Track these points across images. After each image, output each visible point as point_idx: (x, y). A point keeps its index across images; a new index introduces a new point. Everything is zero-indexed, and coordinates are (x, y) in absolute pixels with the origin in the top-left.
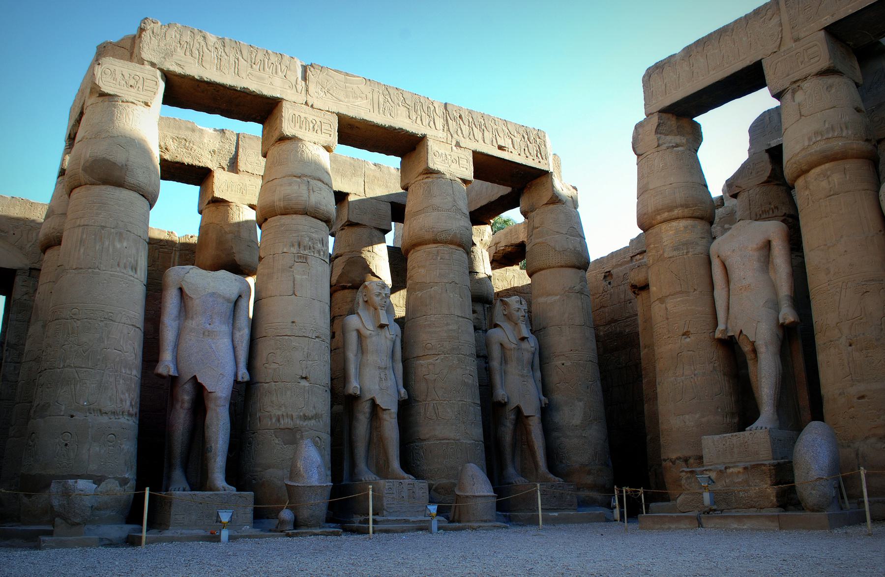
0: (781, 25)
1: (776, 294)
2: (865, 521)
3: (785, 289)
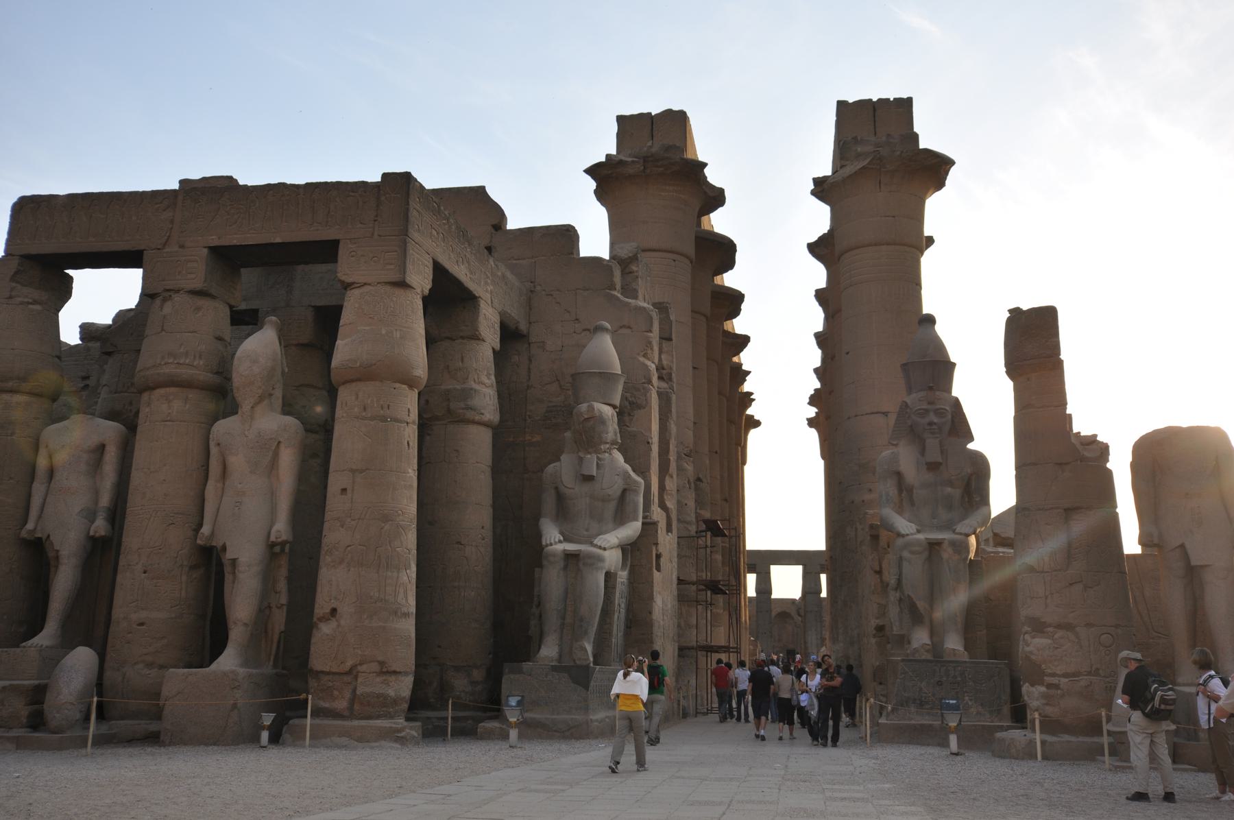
0: (172, 222)
1: (96, 502)
2: (86, 746)
3: (105, 500)
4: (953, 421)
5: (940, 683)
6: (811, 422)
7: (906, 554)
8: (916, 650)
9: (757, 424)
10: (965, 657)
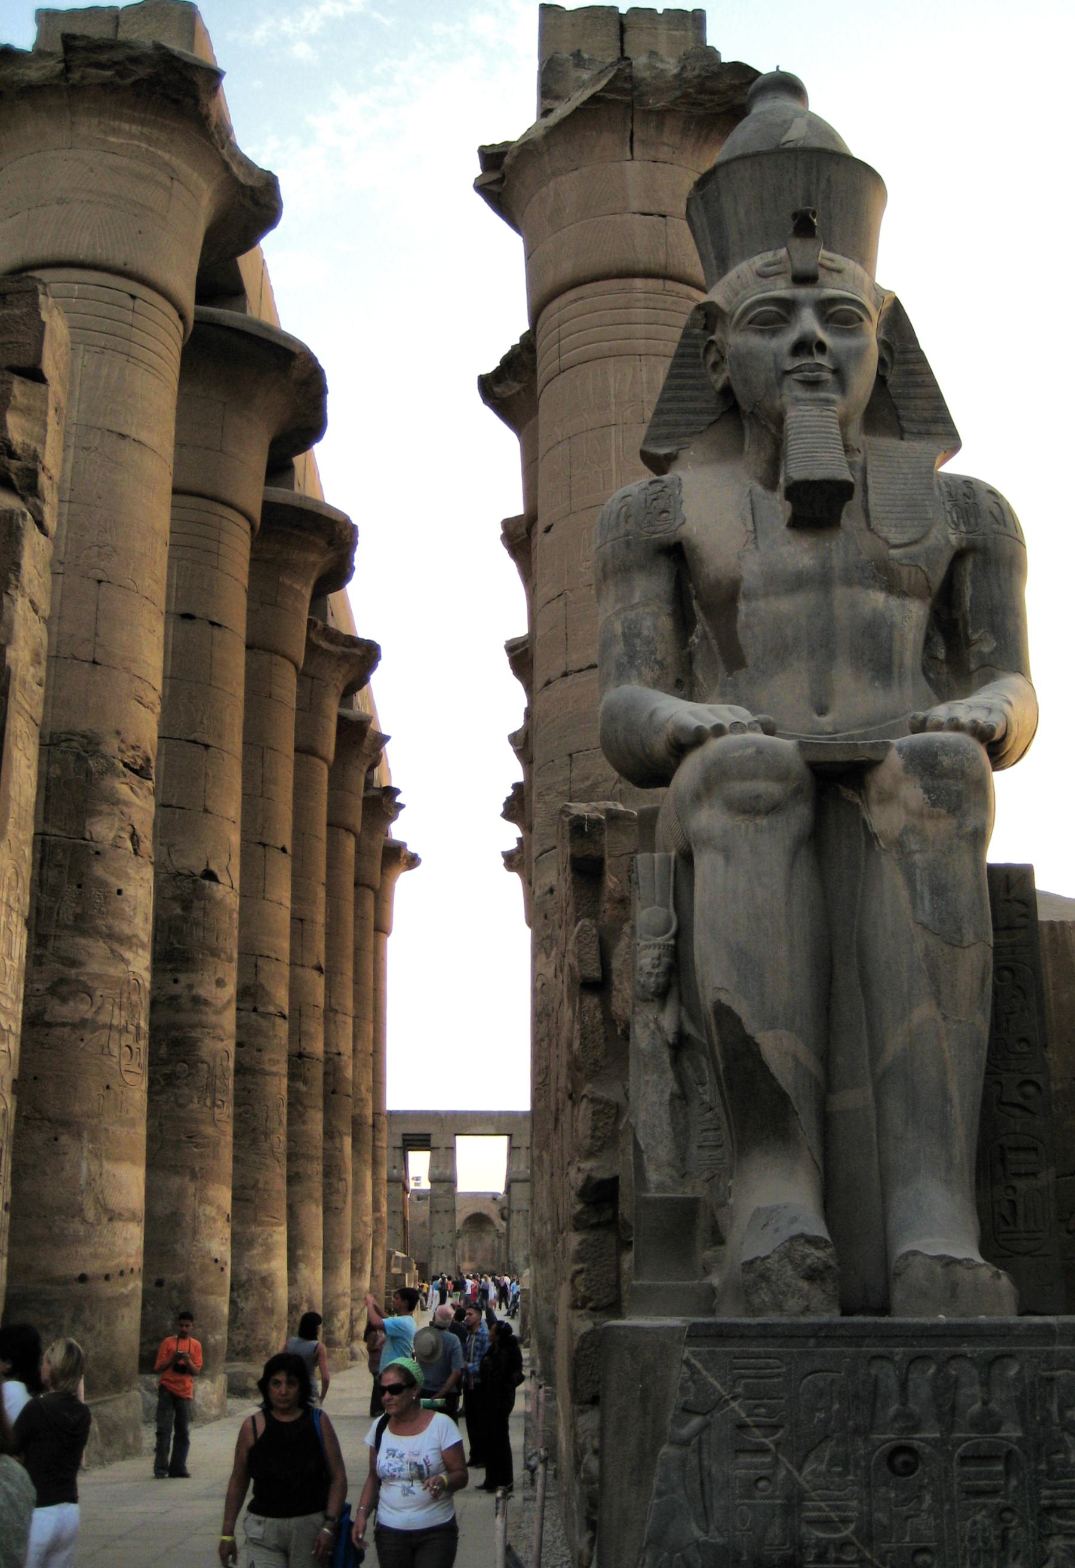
4: (881, 380)
5: (902, 1460)
6: (512, 861)
7: (709, 819)
8: (756, 1272)
9: (413, 861)
10: (994, 1298)
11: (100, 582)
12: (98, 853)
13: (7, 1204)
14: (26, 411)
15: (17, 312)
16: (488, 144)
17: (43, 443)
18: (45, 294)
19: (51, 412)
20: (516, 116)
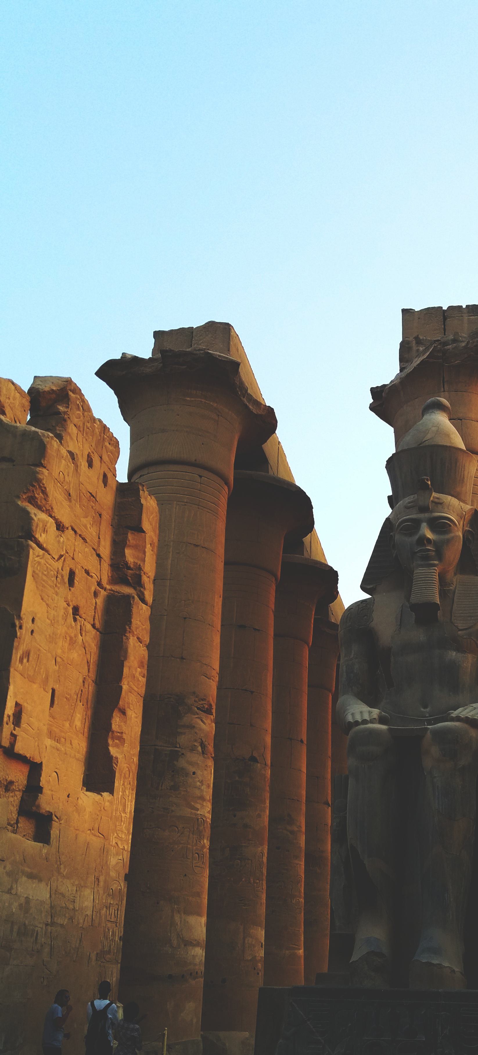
11: (185, 618)
12: (183, 754)
13: (121, 937)
14: (136, 547)
15: (130, 500)
16: (375, 386)
17: (144, 561)
18: (143, 490)
19: (148, 546)
20: (388, 371)
